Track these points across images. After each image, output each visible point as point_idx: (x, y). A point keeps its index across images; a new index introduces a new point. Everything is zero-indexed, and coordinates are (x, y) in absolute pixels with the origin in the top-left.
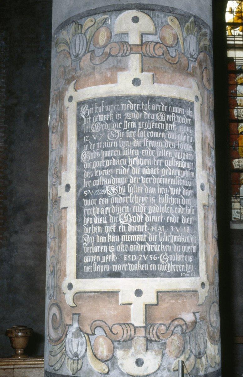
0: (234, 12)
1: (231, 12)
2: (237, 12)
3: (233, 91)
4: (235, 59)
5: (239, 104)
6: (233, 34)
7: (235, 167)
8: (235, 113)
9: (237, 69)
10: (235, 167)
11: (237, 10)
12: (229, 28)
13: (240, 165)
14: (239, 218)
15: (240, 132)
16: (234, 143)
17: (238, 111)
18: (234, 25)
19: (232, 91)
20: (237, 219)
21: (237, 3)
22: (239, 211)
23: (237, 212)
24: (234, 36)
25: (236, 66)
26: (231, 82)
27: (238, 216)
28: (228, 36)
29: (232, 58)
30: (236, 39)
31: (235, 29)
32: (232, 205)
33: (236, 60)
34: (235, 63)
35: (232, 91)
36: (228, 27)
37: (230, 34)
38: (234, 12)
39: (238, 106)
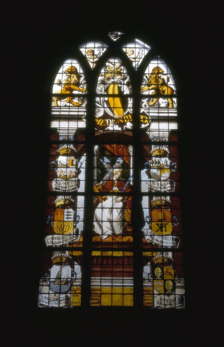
0: (62, 84)
1: (60, 84)
2: (65, 84)
3: (54, 162)
4: (59, 130)
5: (58, 176)
6: (59, 105)
7: (47, 245)
8: (54, 184)
9: (60, 139)
10: (47, 245)
11: (66, 82)
12: (55, 100)
13: (54, 243)
14: (47, 304)
15: (57, 205)
16: (49, 218)
17: (56, 183)
18: (61, 97)
19: (52, 162)
20: (44, 305)
21: (67, 75)
22: (47, 296)
23: (45, 298)
24: (60, 106)
25: (59, 136)
26: (53, 153)
27: (46, 302)
28: (54, 107)
29: (57, 128)
30: (61, 110)
31: (62, 100)
32: (40, 289)
33: (60, 131)
34: (58, 133)
35: (52, 162)
36: (54, 98)
37: (55, 105)
38: (62, 84)
39: (58, 178)
